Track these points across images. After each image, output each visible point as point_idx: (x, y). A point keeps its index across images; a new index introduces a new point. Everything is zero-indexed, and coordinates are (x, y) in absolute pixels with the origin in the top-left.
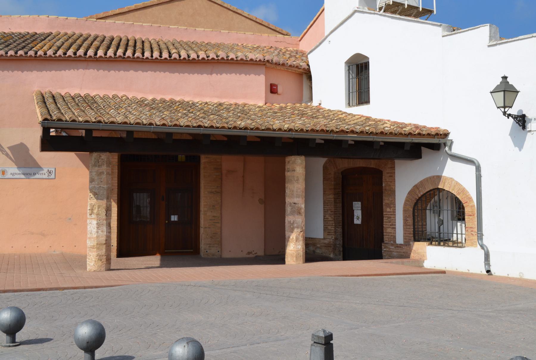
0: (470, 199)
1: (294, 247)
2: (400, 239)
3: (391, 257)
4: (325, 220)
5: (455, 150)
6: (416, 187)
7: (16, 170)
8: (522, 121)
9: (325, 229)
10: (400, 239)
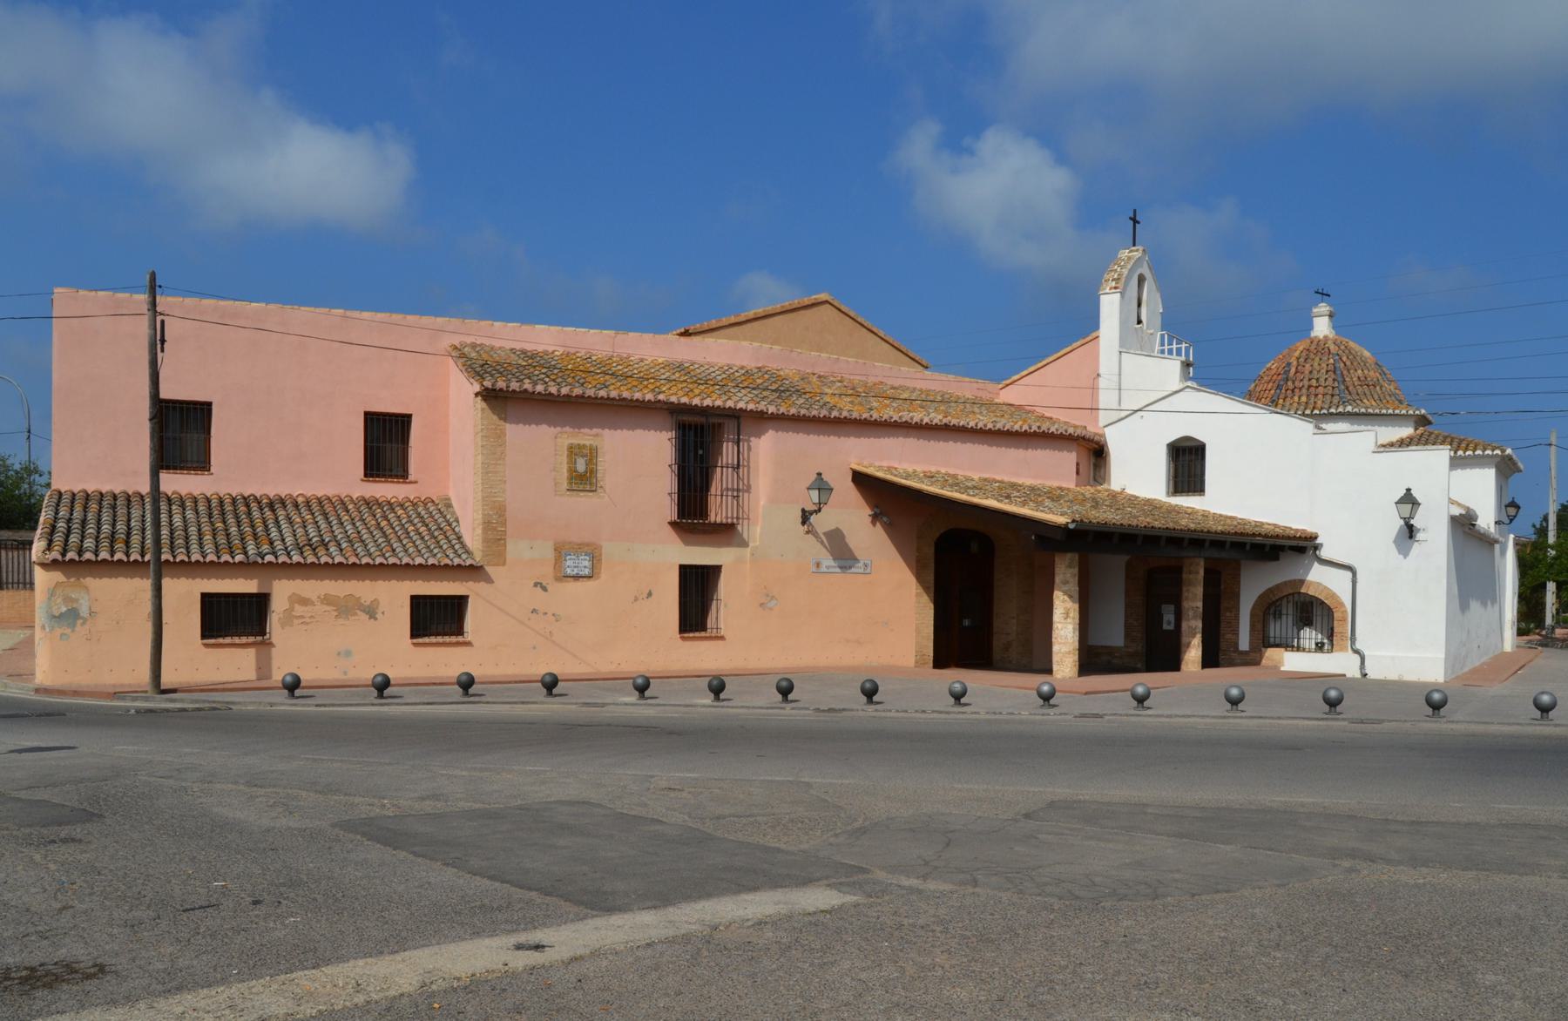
0: (1342, 604)
1: (1193, 654)
2: (1244, 643)
3: (1231, 664)
4: (1127, 627)
5: (1324, 553)
6: (1270, 590)
7: (832, 563)
8: (1410, 531)
9: (1127, 635)
10: (1244, 643)
